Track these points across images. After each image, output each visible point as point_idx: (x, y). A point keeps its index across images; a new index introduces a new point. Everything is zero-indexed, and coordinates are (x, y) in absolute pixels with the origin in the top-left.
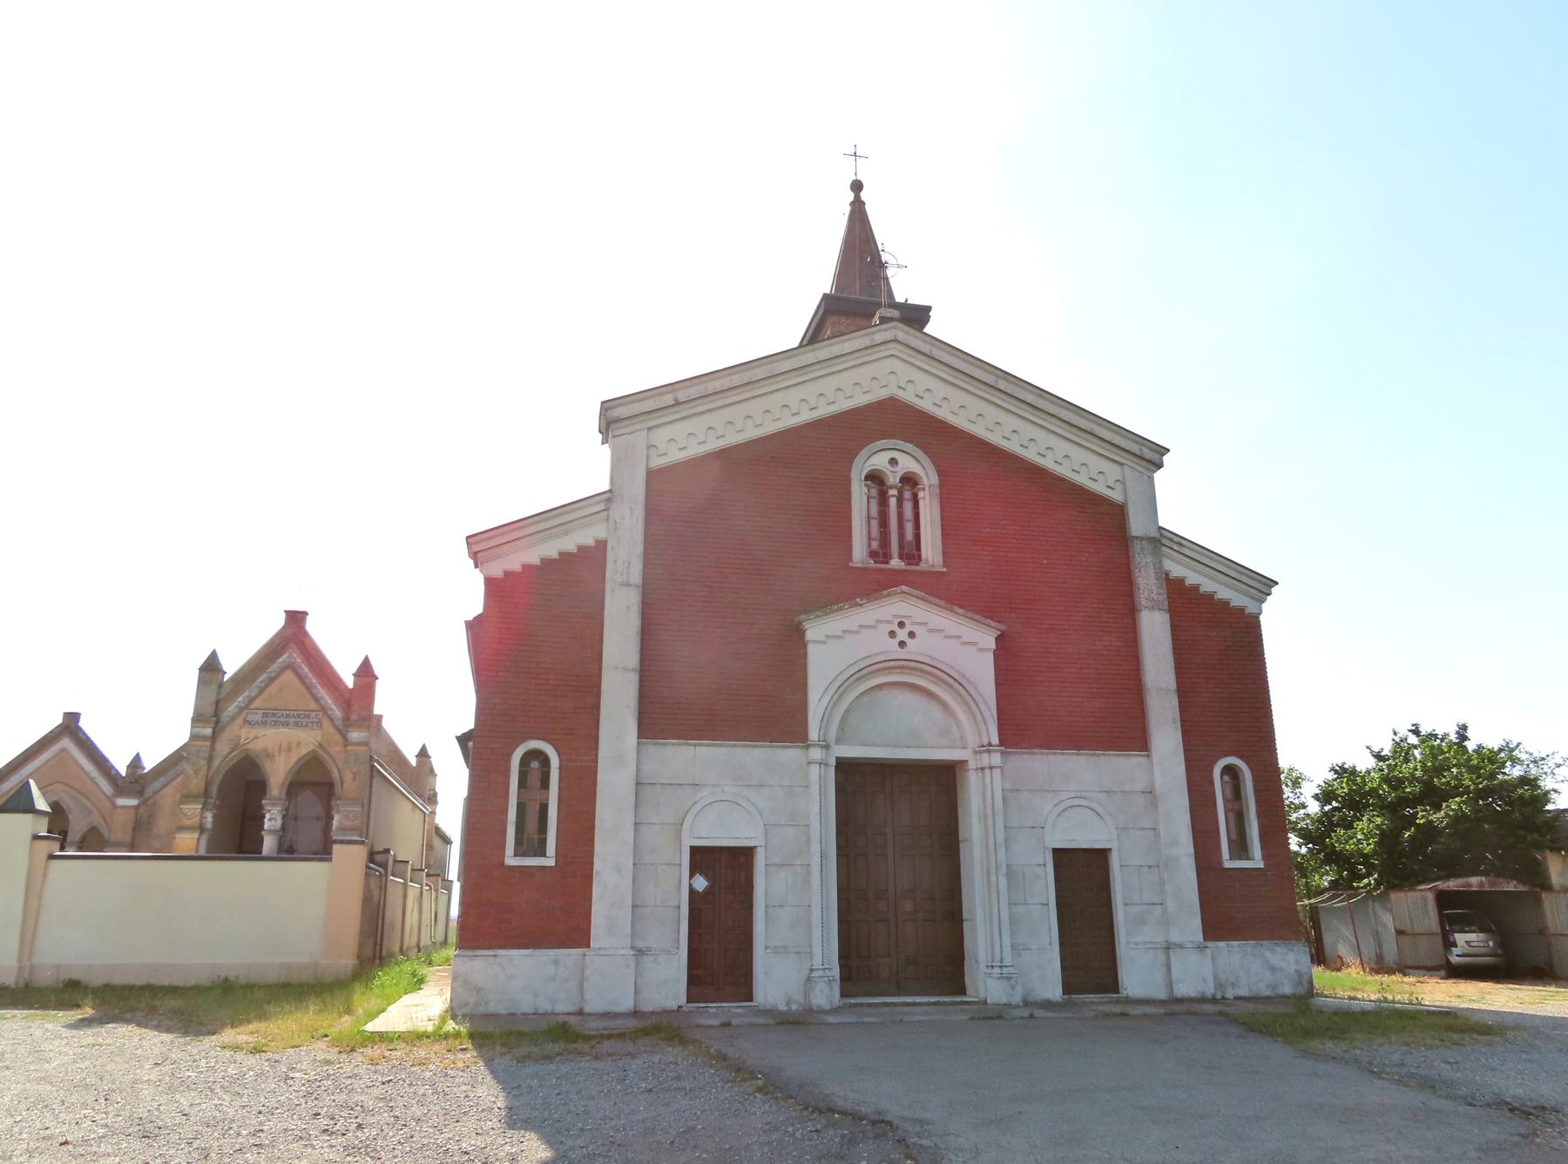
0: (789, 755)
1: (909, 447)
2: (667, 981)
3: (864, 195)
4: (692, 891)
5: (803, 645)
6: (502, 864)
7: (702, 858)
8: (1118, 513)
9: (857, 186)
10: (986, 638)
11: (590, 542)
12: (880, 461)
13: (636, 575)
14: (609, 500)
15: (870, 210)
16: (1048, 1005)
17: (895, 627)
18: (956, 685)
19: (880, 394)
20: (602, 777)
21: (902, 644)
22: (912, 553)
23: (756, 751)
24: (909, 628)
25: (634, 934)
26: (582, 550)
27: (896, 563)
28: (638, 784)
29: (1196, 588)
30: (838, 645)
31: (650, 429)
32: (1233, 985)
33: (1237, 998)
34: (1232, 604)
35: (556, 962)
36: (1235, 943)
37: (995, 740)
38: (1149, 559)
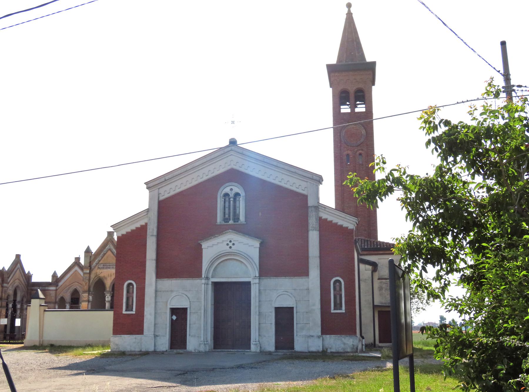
0: (197, 281)
1: (236, 184)
2: (164, 343)
3: (352, 10)
4: (172, 320)
5: (201, 250)
6: (122, 313)
7: (174, 311)
8: (304, 198)
9: (349, 6)
10: (256, 244)
11: (143, 224)
12: (227, 190)
13: (155, 233)
14: (148, 211)
15: (354, 16)
16: (270, 353)
17: (228, 242)
18: (250, 260)
19: (228, 168)
20: (146, 290)
21: (230, 247)
22: (236, 218)
23: (188, 281)
24: (232, 242)
25: (154, 332)
26: (142, 226)
27: (231, 222)
28: (156, 291)
29: (331, 222)
30: (210, 249)
31: (159, 189)
32: (330, 348)
33: (331, 352)
34: (344, 226)
35: (135, 338)
36: (333, 336)
37: (257, 275)
38: (314, 213)
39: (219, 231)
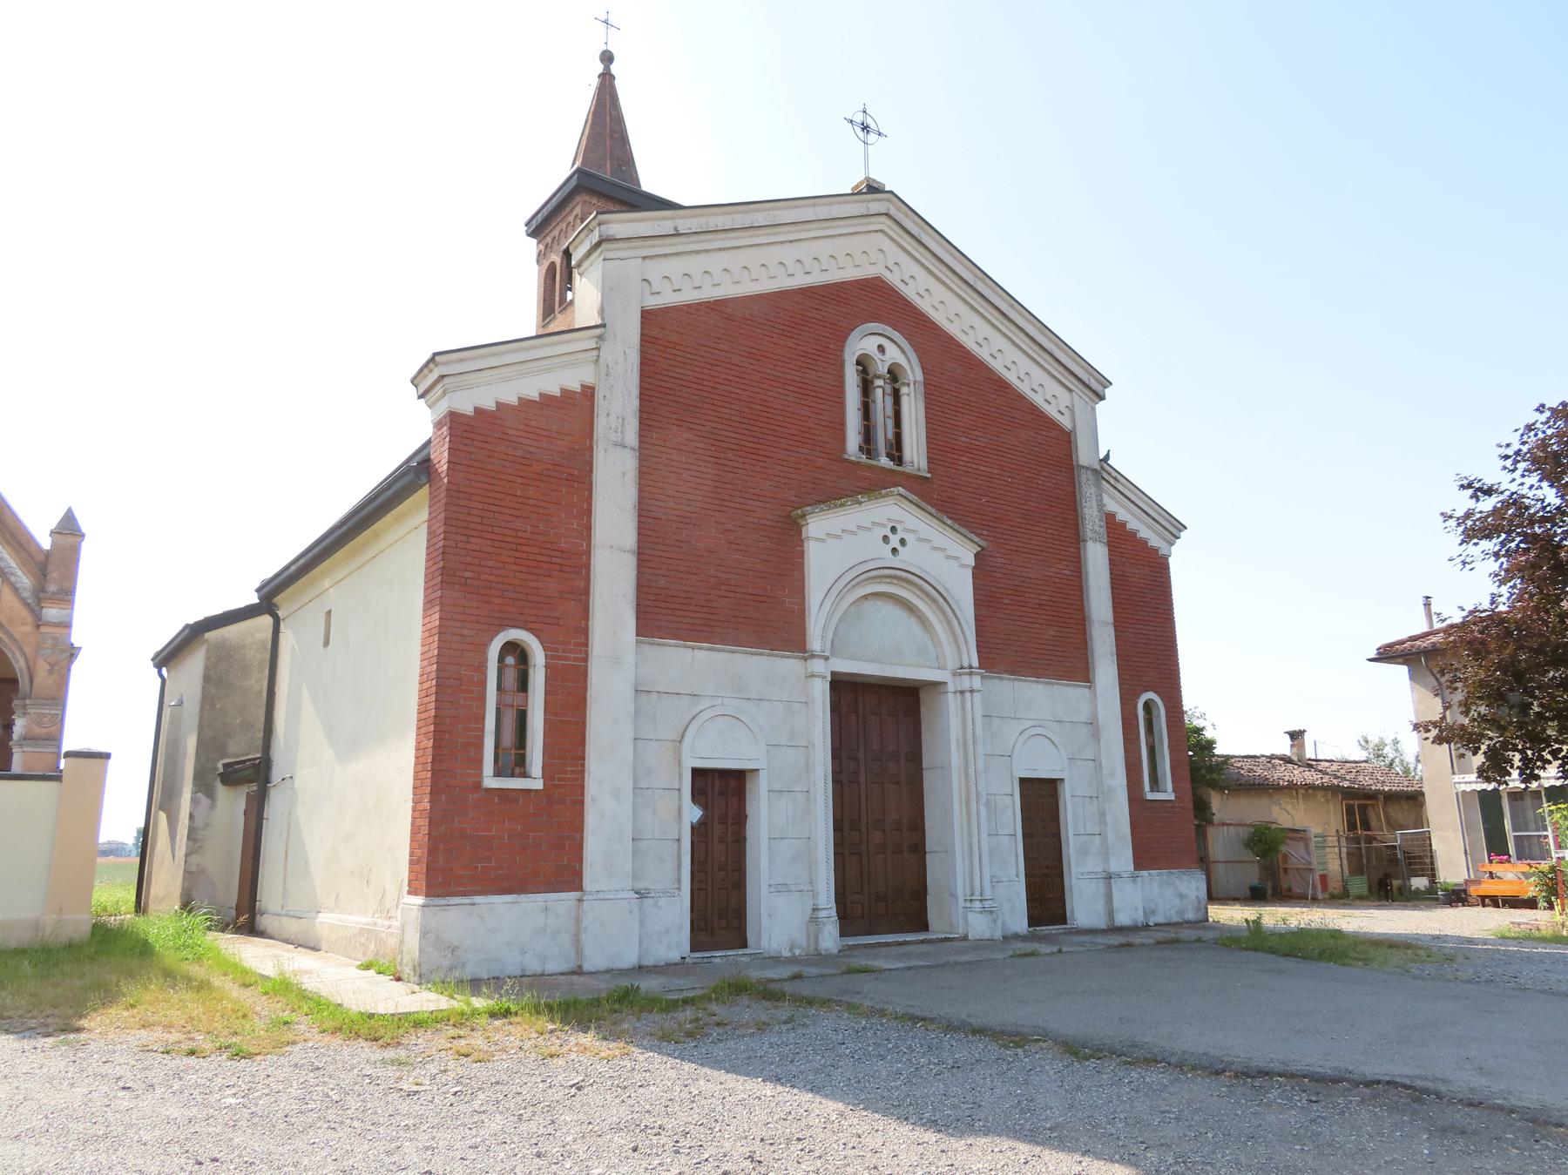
0: (788, 665)
1: (896, 336)
2: (668, 926)
3: (614, 69)
6: (478, 785)
8: (1066, 439)
9: (607, 58)
12: (869, 345)
15: (619, 84)
22: (896, 449)
25: (635, 875)
26: (567, 394)
30: (840, 544)
37: (976, 663)
39: (869, 484)
